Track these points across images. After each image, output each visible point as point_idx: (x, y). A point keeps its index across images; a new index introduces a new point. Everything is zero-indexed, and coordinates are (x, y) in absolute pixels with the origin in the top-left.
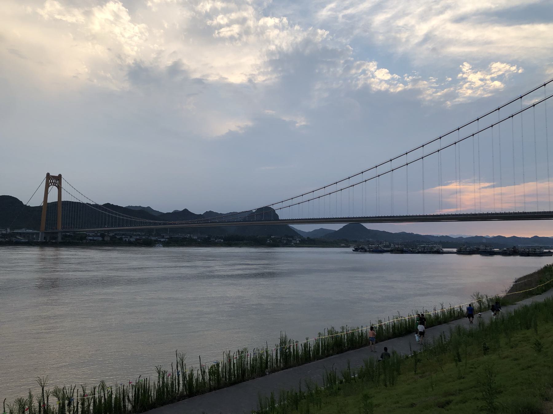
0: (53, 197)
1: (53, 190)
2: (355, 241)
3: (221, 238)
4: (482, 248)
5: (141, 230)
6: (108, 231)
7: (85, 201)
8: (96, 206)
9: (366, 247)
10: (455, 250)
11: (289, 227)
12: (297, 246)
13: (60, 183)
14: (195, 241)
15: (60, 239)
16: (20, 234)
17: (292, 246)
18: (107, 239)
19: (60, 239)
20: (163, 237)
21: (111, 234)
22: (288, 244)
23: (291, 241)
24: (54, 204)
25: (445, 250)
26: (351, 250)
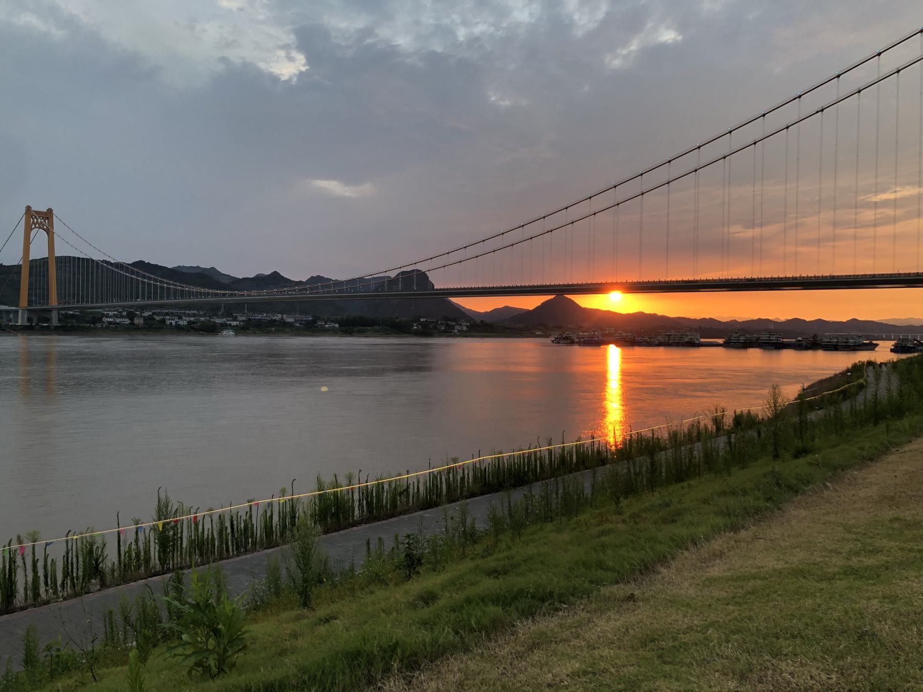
0: (39, 251)
3: (335, 321)
4: (764, 337)
6: (143, 308)
7: (97, 257)
9: (574, 337)
10: (721, 341)
11: (450, 302)
12: (463, 334)
14: (291, 325)
15: (55, 322)
17: (455, 336)
18: (136, 321)
20: (235, 319)
21: (146, 314)
22: (448, 332)
23: (453, 326)
24: (44, 262)
25: (702, 340)
26: (548, 341)
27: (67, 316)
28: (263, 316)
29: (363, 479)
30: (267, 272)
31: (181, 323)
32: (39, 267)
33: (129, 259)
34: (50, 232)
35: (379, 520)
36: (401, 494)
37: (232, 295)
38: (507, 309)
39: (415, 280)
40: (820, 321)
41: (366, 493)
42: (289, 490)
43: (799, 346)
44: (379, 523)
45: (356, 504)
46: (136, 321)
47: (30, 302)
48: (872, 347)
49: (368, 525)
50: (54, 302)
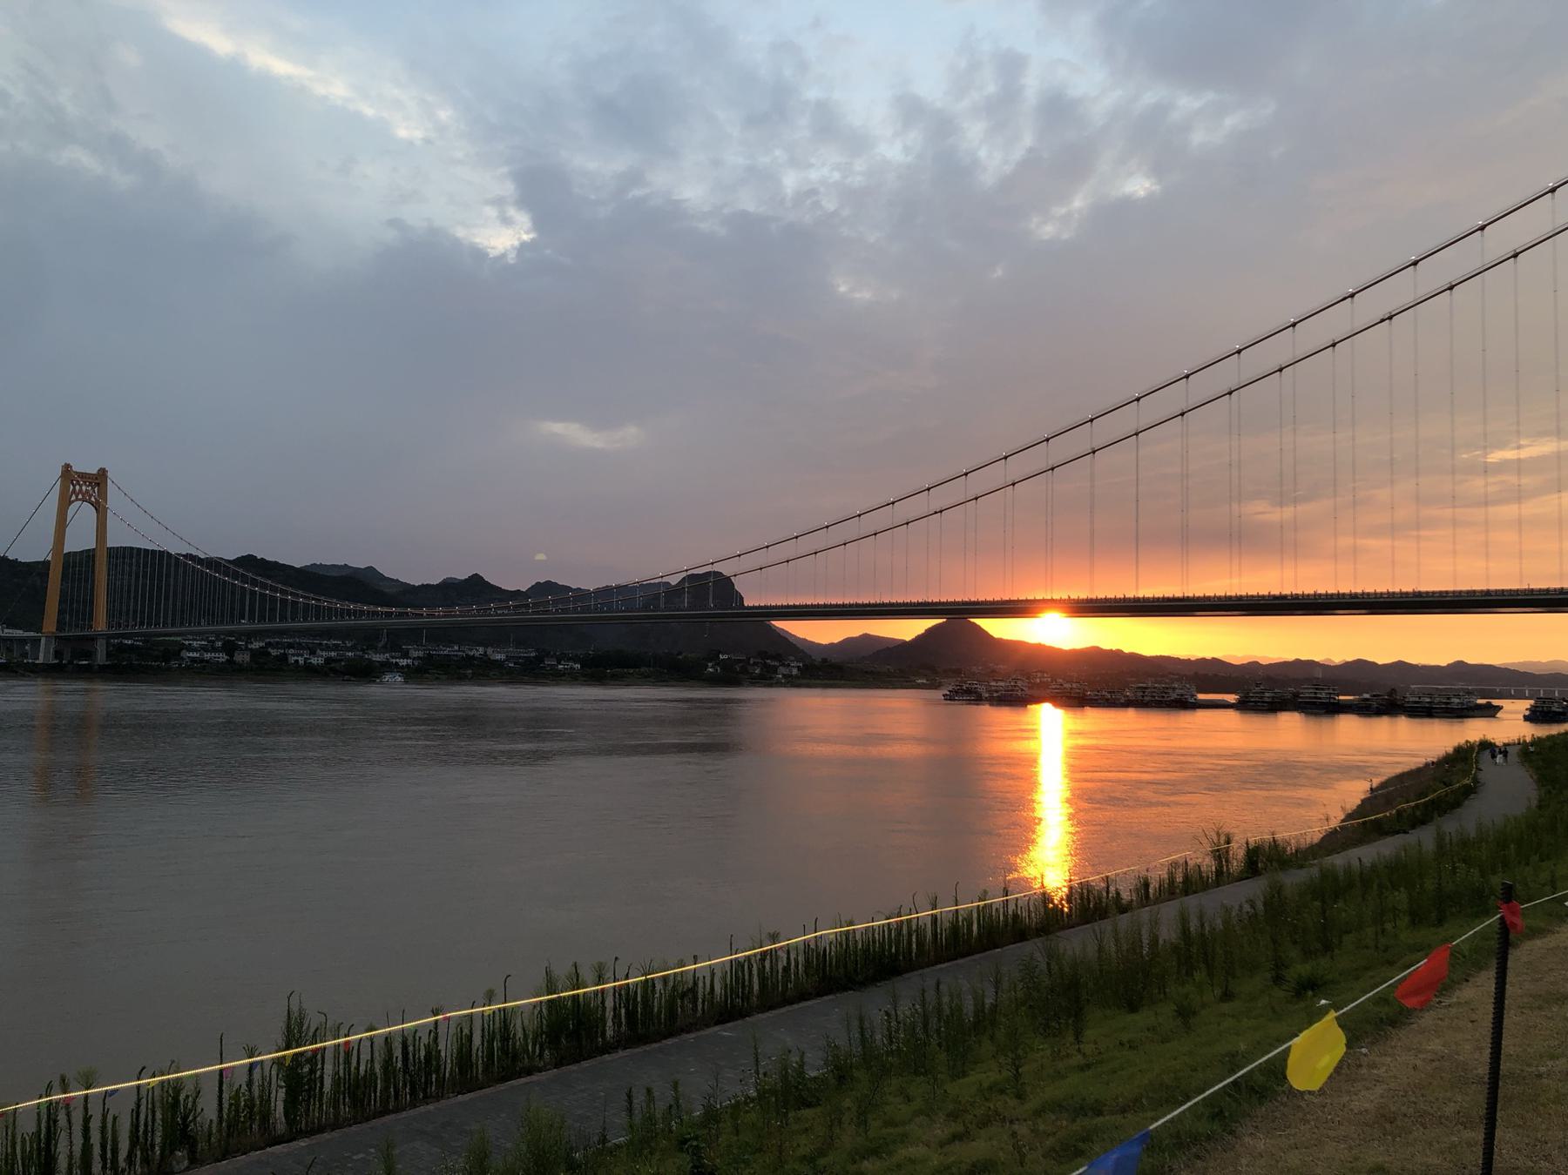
0: (80, 538)
2: (958, 672)
3: (575, 659)
4: (1307, 693)
5: (345, 634)
6: (250, 635)
7: (175, 548)
9: (982, 689)
10: (1231, 698)
12: (792, 682)
13: (103, 494)
15: (101, 658)
17: (779, 684)
18: (240, 657)
19: (101, 658)
20: (406, 655)
21: (256, 645)
22: (767, 679)
23: (775, 670)
24: (88, 556)
25: (1201, 697)
26: (938, 694)
27: (121, 648)
28: (454, 650)
31: (314, 661)
32: (78, 566)
34: (100, 509)
37: (401, 615)
38: (866, 637)
39: (710, 591)
40: (1400, 666)
43: (1365, 710)
48: (1490, 712)
50: (101, 624)
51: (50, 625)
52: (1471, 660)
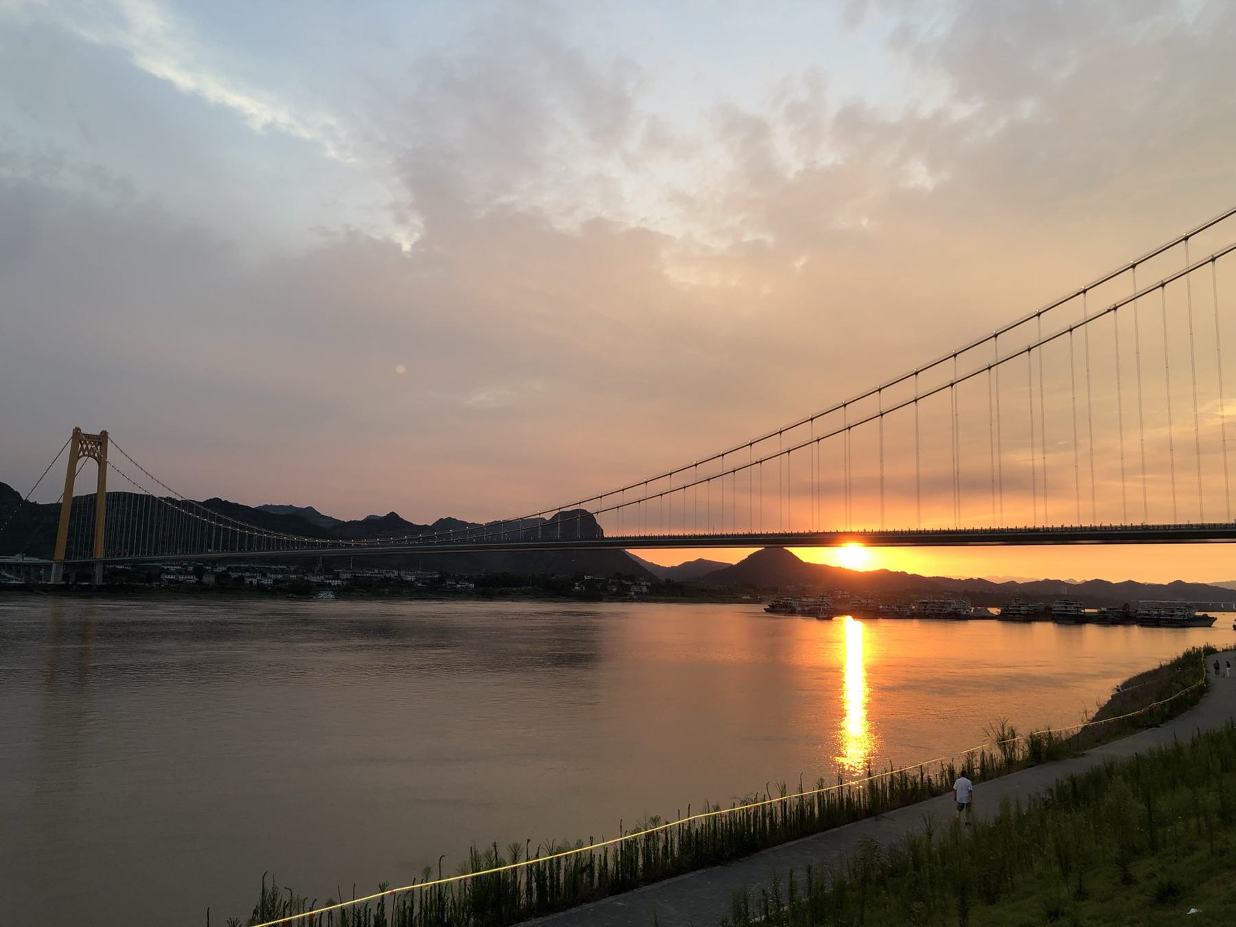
0: (86, 485)
1: (88, 466)
2: (775, 590)
3: (469, 580)
6: (214, 562)
7: (159, 492)
8: (188, 505)
9: (795, 603)
10: (995, 611)
12: (642, 598)
14: (410, 585)
15: (98, 580)
16: (10, 567)
17: (632, 600)
18: (206, 579)
19: (98, 580)
20: (337, 577)
21: (219, 569)
22: (622, 596)
23: (628, 588)
24: (90, 500)
26: (760, 608)
27: (115, 572)
29: (532, 853)
30: (382, 514)
31: (265, 582)
32: (83, 507)
33: (200, 495)
34: (102, 462)
35: (554, 912)
36: (583, 870)
37: (334, 545)
38: (700, 562)
39: (577, 524)
40: (1130, 584)
41: (537, 872)
42: (435, 870)
43: (1104, 620)
44: (555, 916)
45: (523, 887)
46: (206, 579)
47: (68, 554)
49: (539, 920)
50: (99, 552)
51: (60, 554)
52: (1188, 580)
